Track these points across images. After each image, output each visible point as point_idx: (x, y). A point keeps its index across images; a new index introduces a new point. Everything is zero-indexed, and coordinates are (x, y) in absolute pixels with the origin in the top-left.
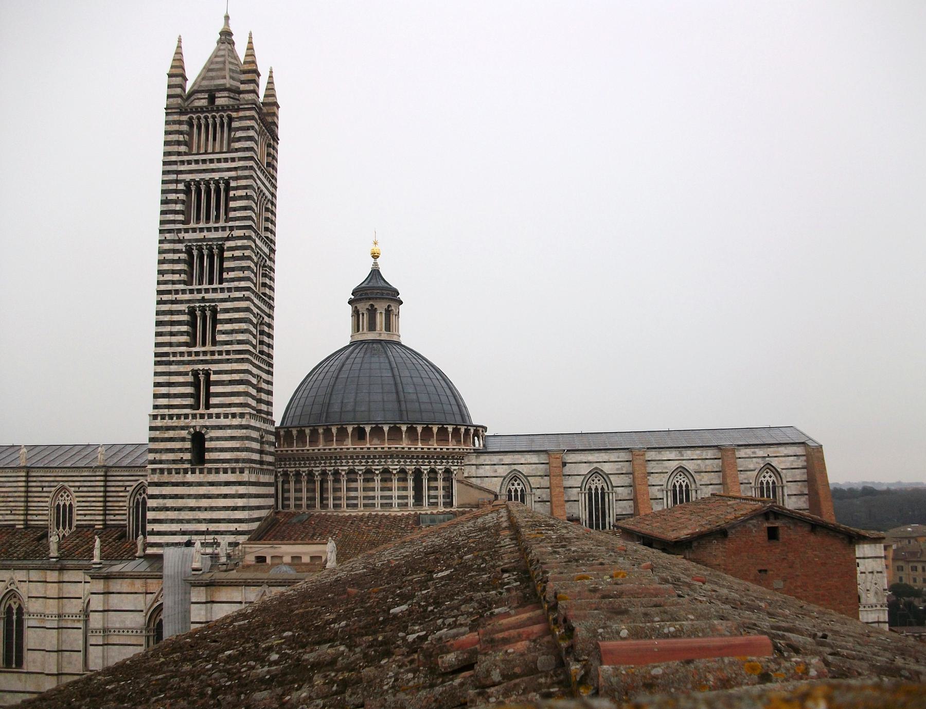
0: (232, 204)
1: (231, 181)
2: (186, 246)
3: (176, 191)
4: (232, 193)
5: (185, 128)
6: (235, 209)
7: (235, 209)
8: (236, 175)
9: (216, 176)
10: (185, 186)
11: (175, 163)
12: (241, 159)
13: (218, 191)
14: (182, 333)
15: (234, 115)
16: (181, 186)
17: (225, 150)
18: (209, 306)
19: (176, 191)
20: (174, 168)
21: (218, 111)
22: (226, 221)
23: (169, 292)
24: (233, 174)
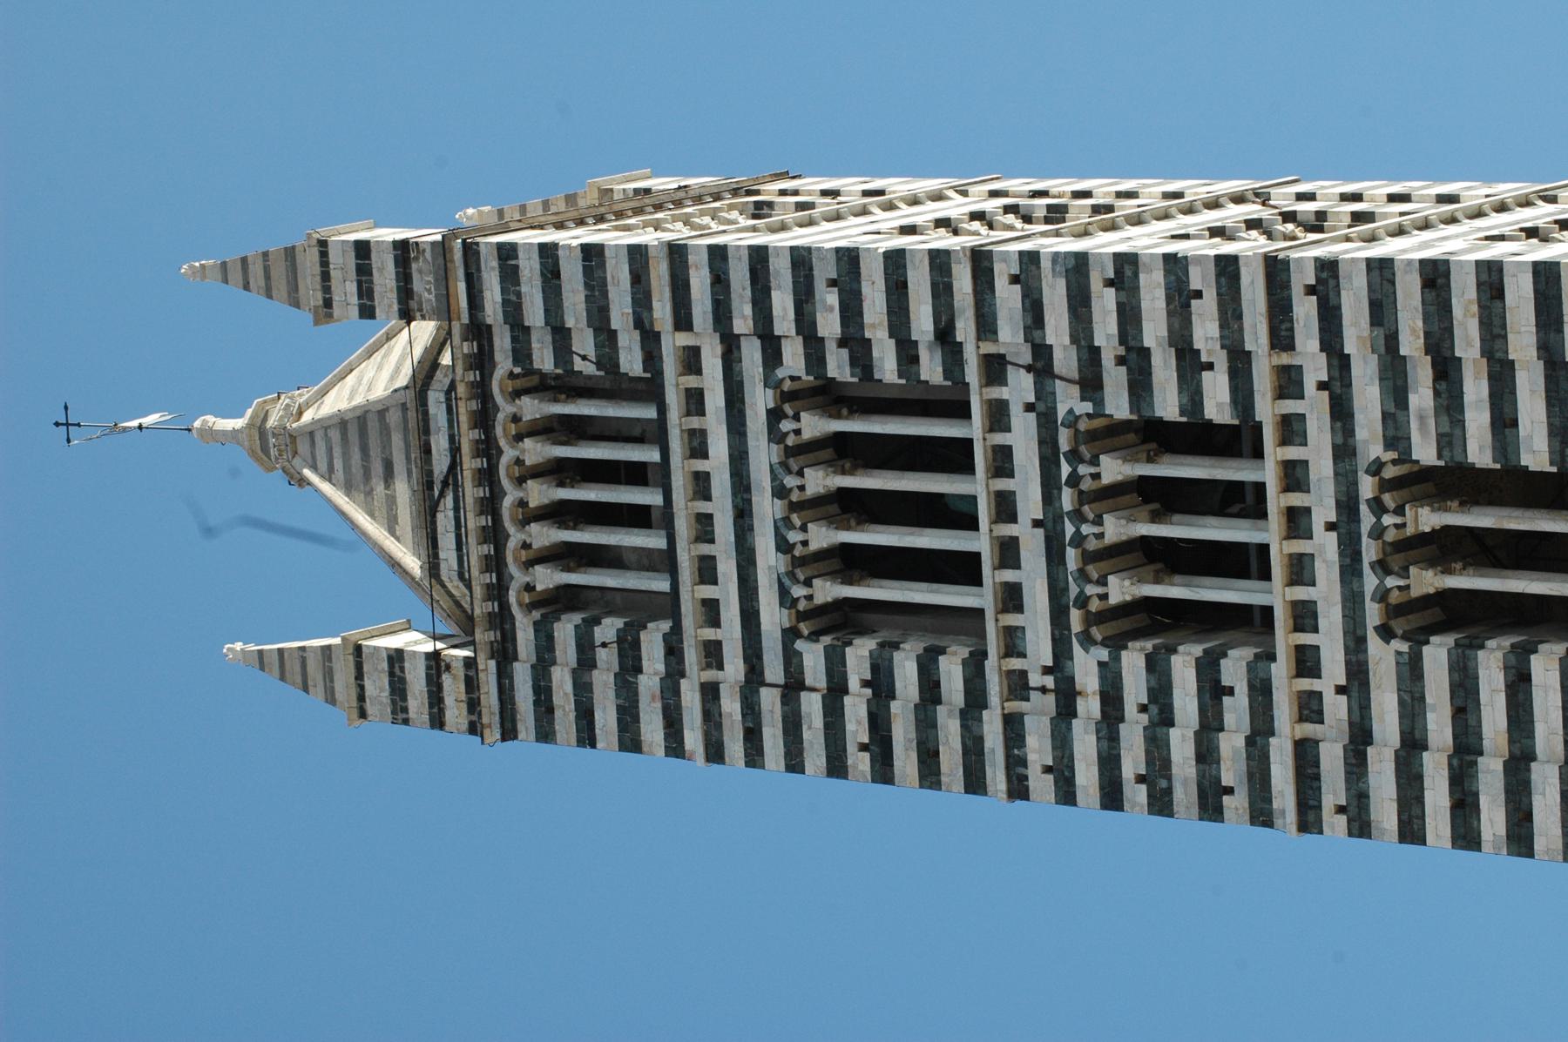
0: (887, 365)
1: (780, 373)
2: (1087, 641)
3: (836, 690)
4: (838, 366)
5: (565, 630)
6: (908, 354)
7: (908, 354)
8: (757, 343)
9: (762, 455)
10: (814, 636)
11: (710, 692)
12: (683, 321)
13: (844, 451)
14: (1519, 684)
15: (504, 364)
16: (813, 657)
17: (650, 413)
18: (1378, 507)
19: (836, 690)
20: (731, 706)
21: (487, 449)
22: (961, 411)
23: (1306, 756)
24: (751, 354)
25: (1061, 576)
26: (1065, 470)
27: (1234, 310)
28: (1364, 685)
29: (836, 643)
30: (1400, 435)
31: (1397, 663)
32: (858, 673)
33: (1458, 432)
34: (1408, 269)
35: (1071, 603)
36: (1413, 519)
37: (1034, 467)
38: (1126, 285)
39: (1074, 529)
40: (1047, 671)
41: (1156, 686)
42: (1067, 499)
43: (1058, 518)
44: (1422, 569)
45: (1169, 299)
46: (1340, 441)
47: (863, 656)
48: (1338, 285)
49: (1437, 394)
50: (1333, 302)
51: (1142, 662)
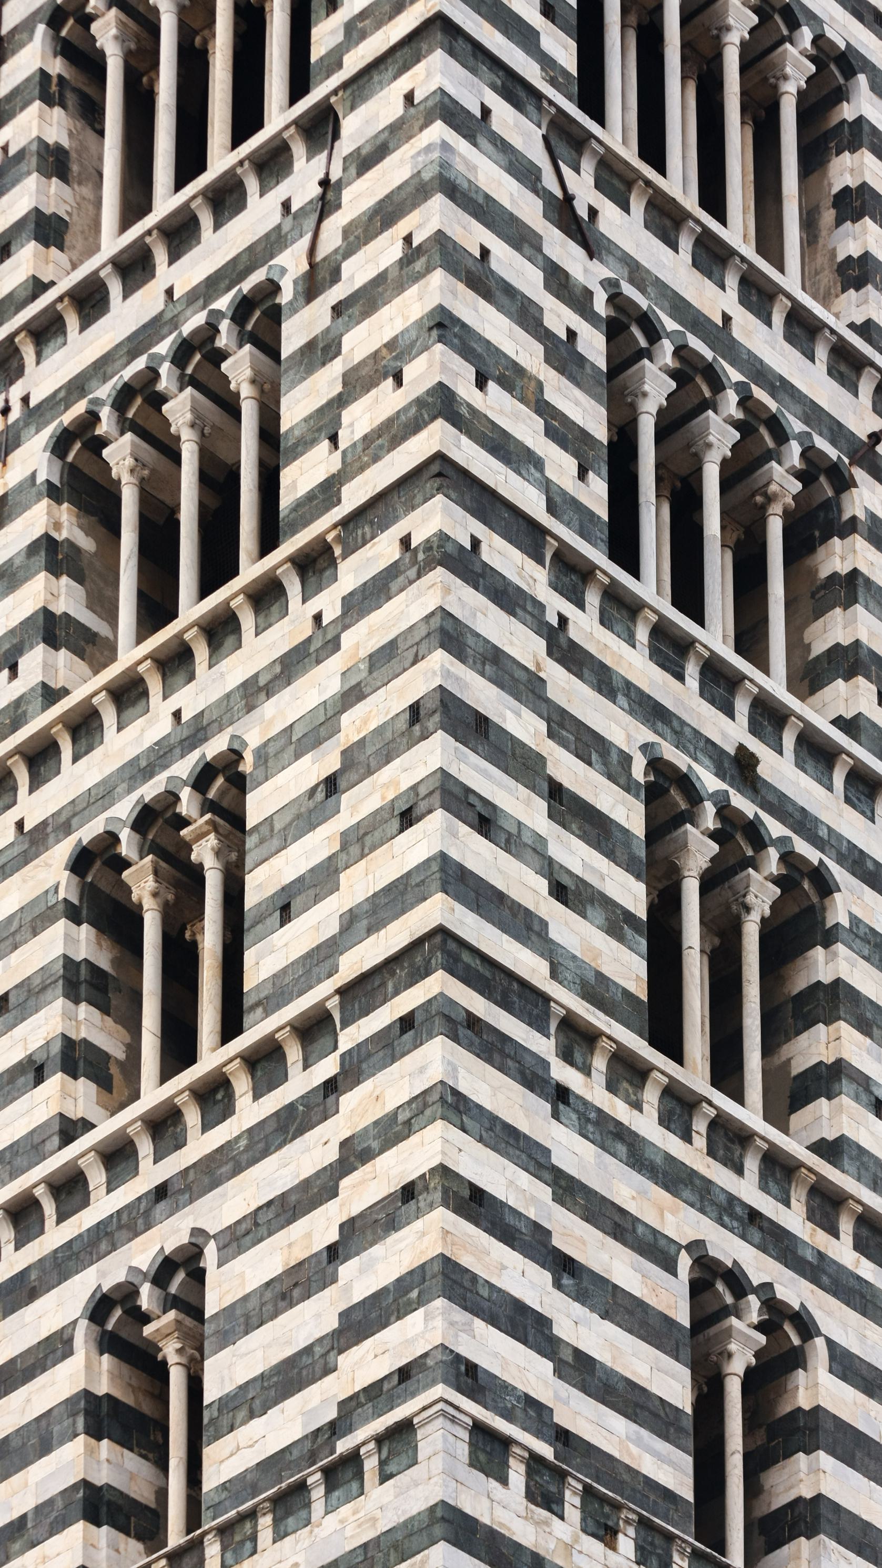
25: (118, 363)
26: (223, 303)
27: (381, 447)
28: (25, 859)
29: (55, 81)
30: (271, 763)
31: (47, 892)
32: (15, 134)
33: (275, 843)
34: (429, 675)
35: (91, 396)
36: (198, 832)
37: (226, 254)
38: (405, 270)
39: (164, 352)
40: (25, 400)
41: (15, 566)
42: (196, 321)
43: (175, 323)
44: (156, 873)
45: (391, 345)
46: (262, 681)
47: (30, 129)
48: (411, 583)
49: (312, 792)
50: (394, 586)
51: (37, 532)
